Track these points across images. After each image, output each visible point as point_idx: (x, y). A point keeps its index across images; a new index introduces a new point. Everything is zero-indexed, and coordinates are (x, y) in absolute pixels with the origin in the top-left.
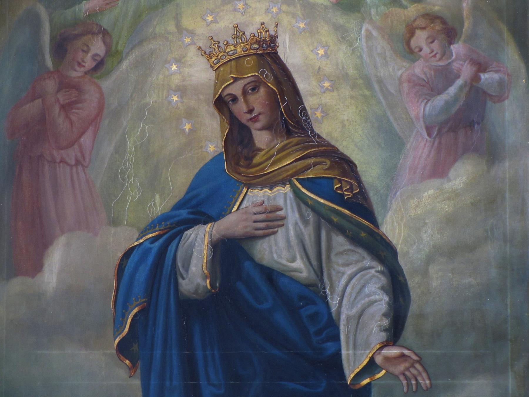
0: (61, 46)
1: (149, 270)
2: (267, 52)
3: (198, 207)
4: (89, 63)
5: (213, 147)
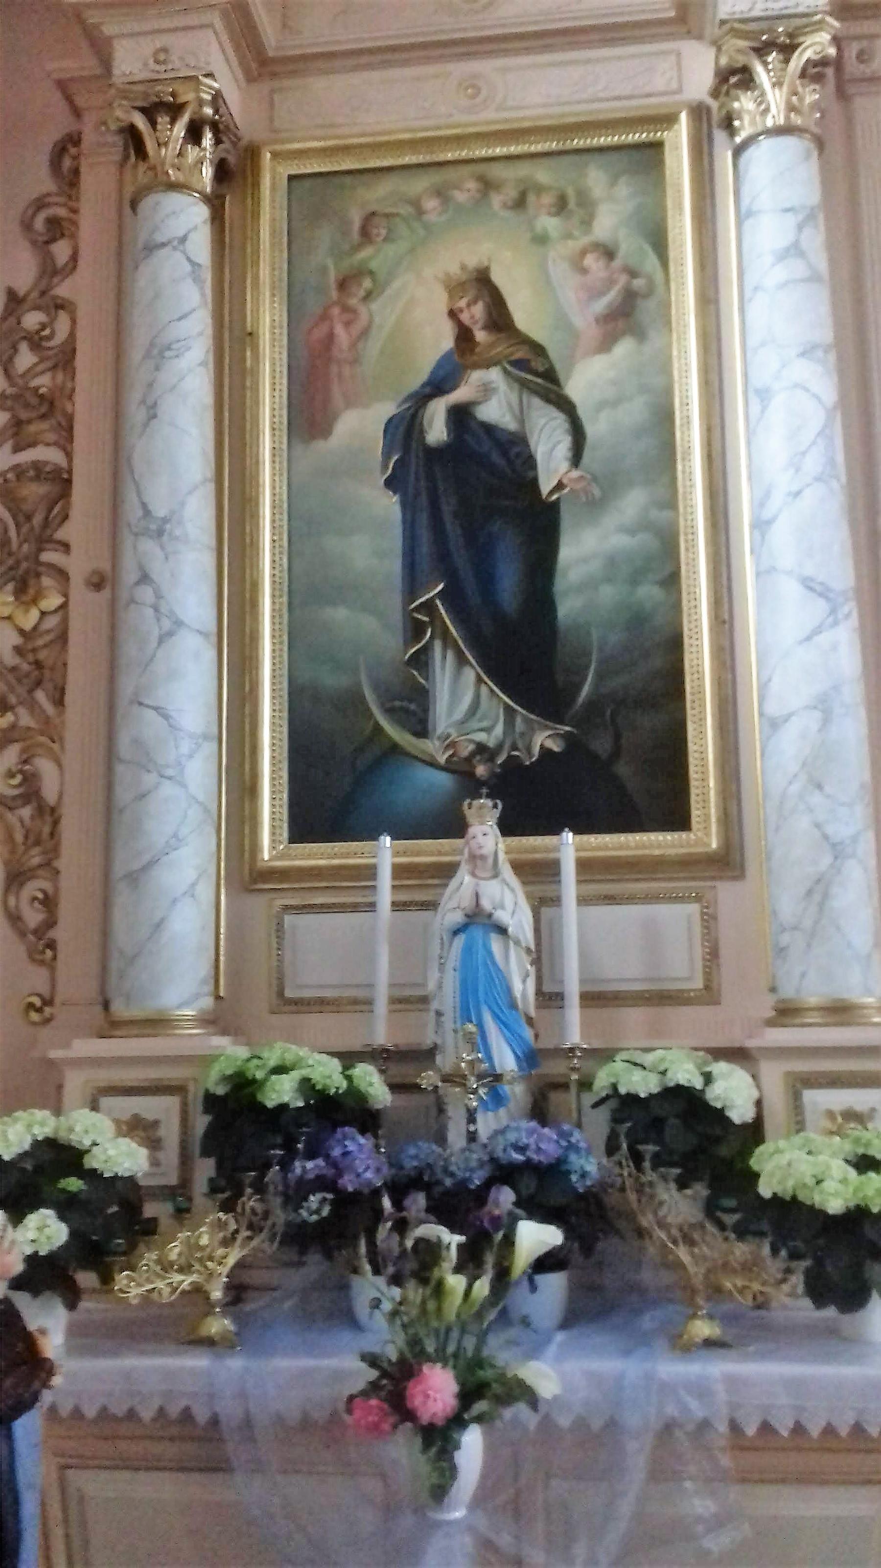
0: (343, 285)
1: (405, 429)
2: (483, 283)
3: (438, 386)
4: (362, 293)
5: (447, 342)
